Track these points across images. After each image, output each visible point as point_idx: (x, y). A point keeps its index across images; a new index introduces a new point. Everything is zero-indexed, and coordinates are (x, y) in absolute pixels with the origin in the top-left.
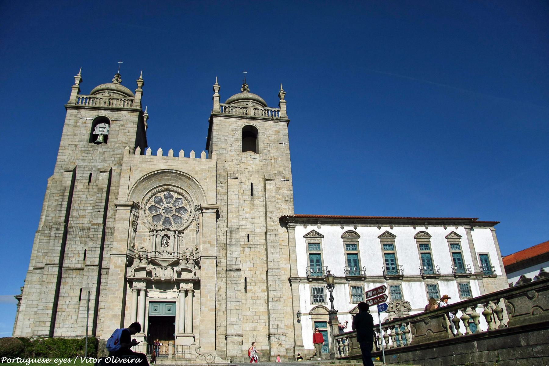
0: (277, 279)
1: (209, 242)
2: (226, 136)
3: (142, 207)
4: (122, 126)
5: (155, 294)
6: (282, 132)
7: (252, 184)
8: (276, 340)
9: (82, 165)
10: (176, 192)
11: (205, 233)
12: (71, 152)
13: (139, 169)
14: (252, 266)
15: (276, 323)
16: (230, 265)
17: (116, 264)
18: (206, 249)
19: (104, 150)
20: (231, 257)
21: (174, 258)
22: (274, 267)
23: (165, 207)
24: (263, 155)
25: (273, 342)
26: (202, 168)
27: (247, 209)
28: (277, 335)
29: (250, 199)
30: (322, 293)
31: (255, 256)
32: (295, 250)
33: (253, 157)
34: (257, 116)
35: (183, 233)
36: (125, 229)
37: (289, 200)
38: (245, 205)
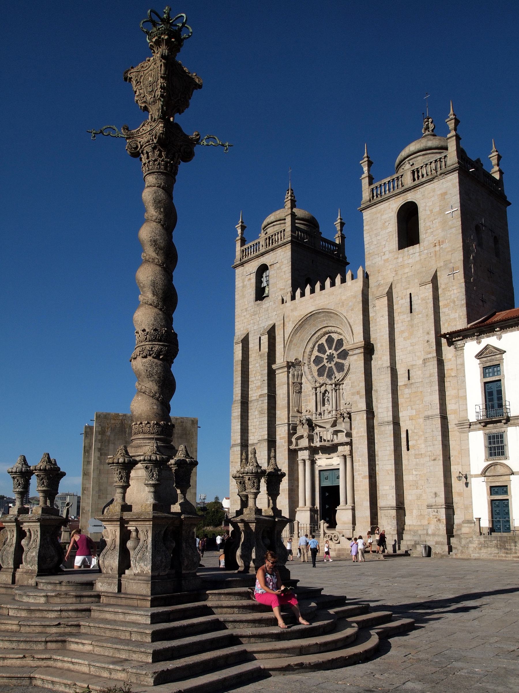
1: (358, 393)
3: (305, 362)
8: (434, 514)
9: (253, 329)
12: (243, 318)
13: (292, 319)
14: (414, 412)
15: (434, 490)
19: (267, 305)
21: (332, 418)
23: (327, 355)
25: (431, 516)
26: (348, 295)
28: (435, 507)
29: (409, 319)
30: (501, 443)
32: (464, 382)
35: (343, 384)
36: (284, 394)
38: (403, 329)
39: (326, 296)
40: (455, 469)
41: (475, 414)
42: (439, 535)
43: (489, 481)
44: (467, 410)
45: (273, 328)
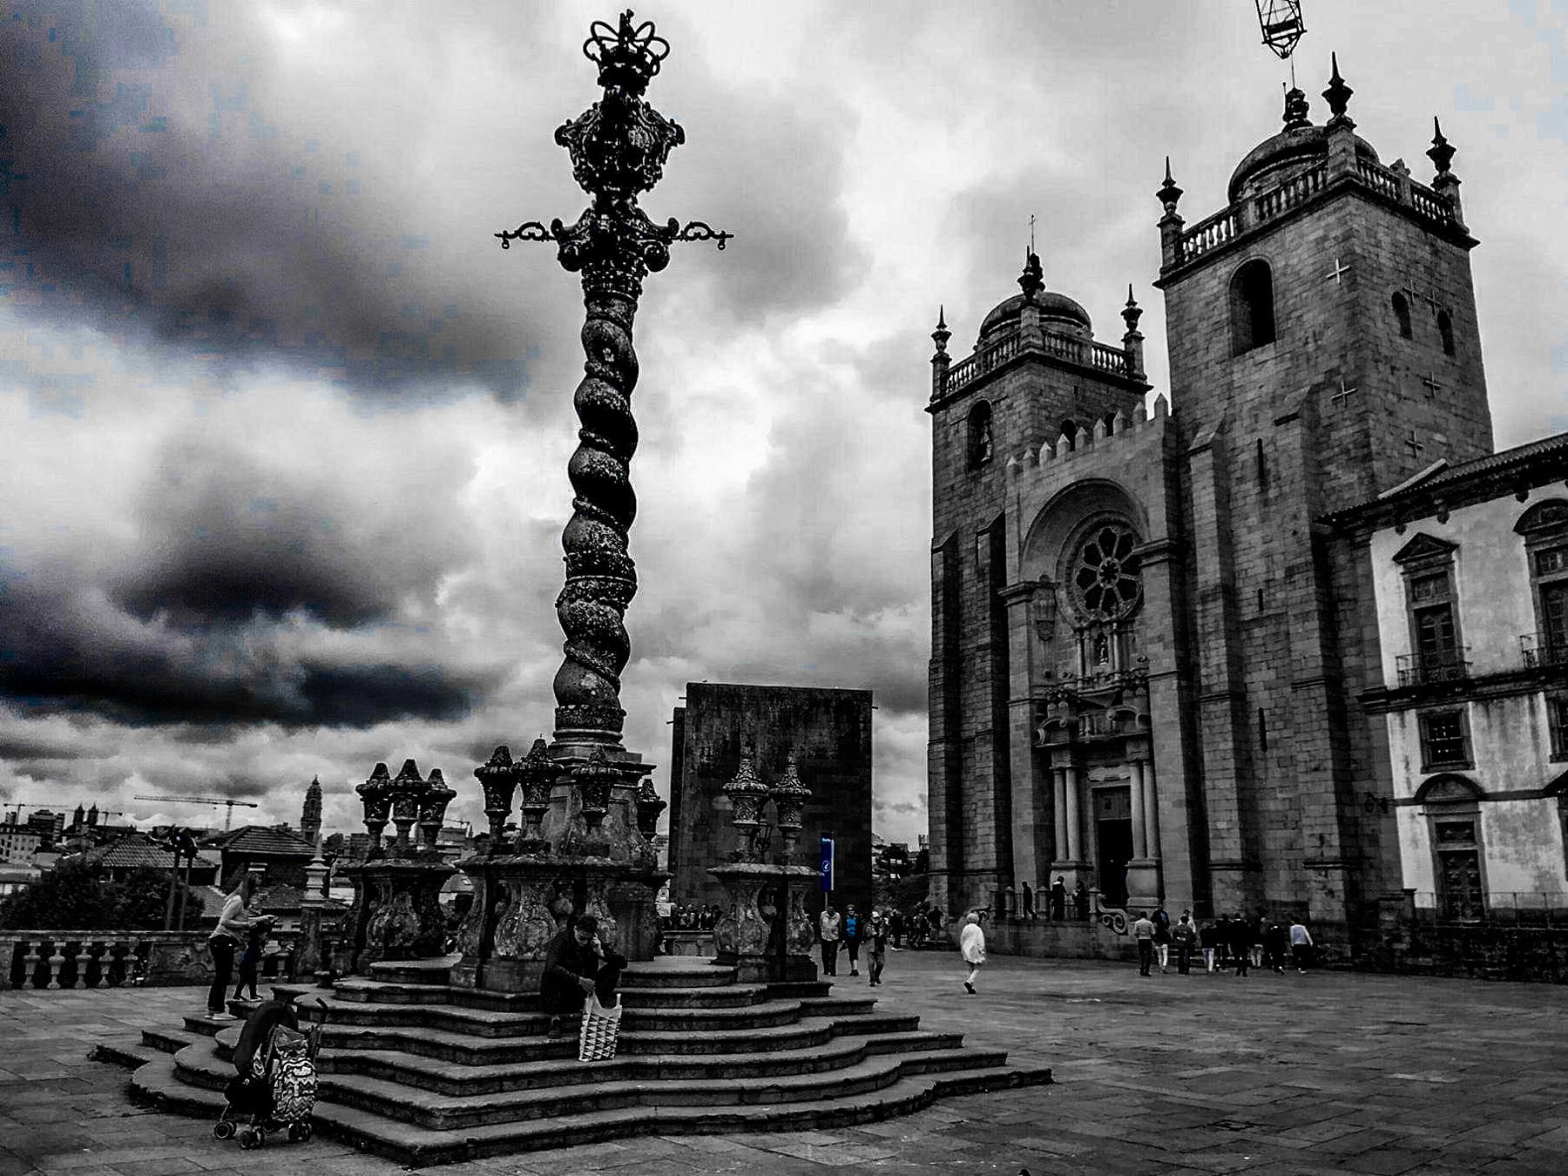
0: (1314, 709)
1: (1160, 638)
2: (1193, 330)
4: (1010, 407)
5: (1099, 774)
6: (1333, 234)
7: (1260, 441)
8: (1320, 879)
10: (1117, 523)
11: (1151, 618)
12: (946, 504)
14: (1272, 674)
15: (1318, 831)
16: (1208, 687)
17: (1016, 721)
18: (1156, 656)
20: (1206, 665)
22: (1305, 675)
23: (1103, 567)
24: (1288, 339)
25: (1313, 884)
27: (1253, 520)
31: (1279, 646)
33: (1259, 358)
34: (1267, 221)
37: (1360, 453)
39: (1096, 454)
40: (1361, 786)
41: (1396, 676)
42: (1331, 924)
43: (1433, 811)
44: (1380, 667)
45: (1001, 521)
